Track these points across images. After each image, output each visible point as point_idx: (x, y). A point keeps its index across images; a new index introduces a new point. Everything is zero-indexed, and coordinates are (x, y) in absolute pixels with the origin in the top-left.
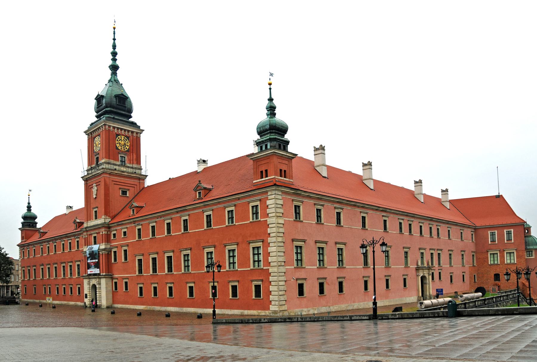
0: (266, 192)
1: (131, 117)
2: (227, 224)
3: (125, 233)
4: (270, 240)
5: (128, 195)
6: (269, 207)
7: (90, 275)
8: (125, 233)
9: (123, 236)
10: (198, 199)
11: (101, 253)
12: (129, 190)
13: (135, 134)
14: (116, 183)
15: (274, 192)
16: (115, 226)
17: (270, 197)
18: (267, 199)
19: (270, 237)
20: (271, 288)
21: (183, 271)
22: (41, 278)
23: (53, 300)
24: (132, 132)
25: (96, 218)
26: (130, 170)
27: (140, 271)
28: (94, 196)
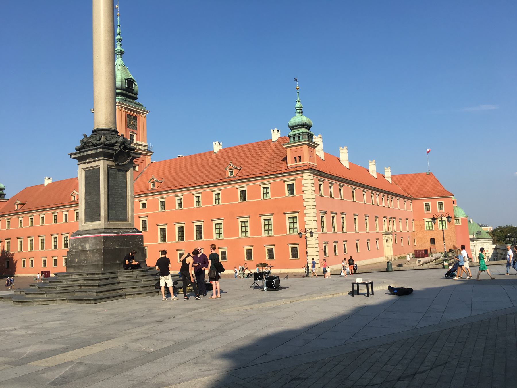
0: (302, 173)
1: (136, 99)
2: (262, 198)
3: (144, 205)
4: (305, 211)
5: (137, 169)
6: (305, 185)
9: (141, 207)
13: (142, 114)
15: (309, 174)
17: (304, 178)
18: (302, 179)
21: (215, 238)
22: (19, 250)
24: (140, 113)
27: (163, 239)
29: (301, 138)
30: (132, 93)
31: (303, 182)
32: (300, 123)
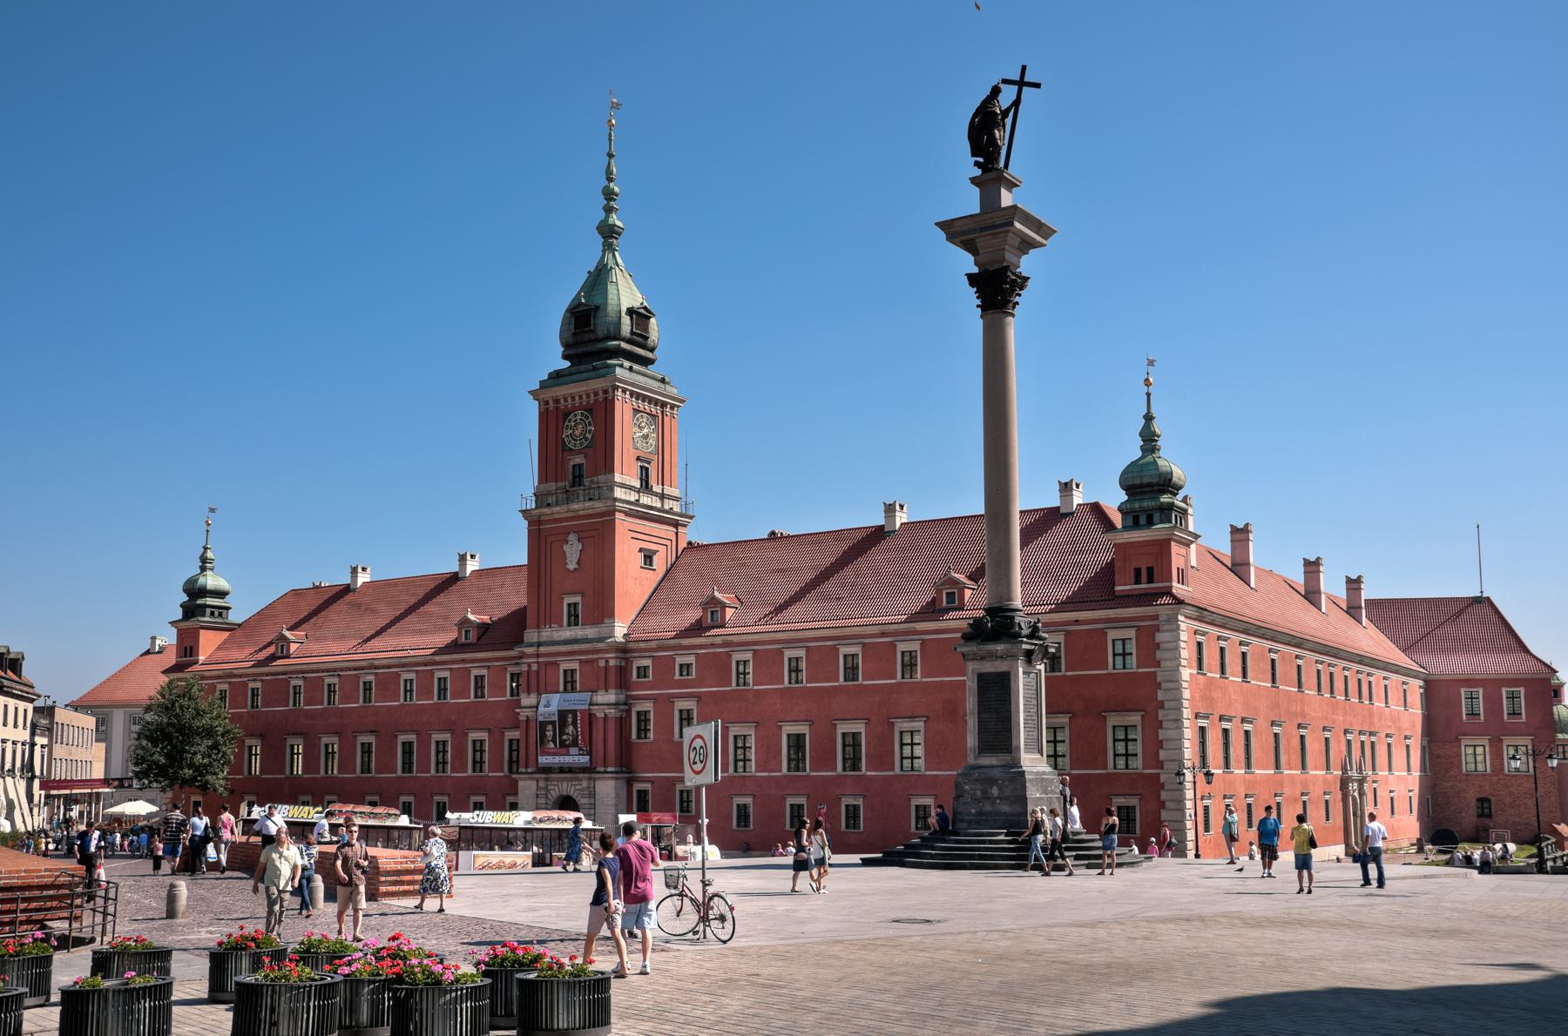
4: (1161, 713)
7: (547, 770)
8: (686, 668)
9: (677, 677)
10: (947, 610)
11: (600, 715)
12: (655, 552)
14: (636, 535)
18: (1157, 629)
19: (1162, 707)
20: (1164, 815)
21: (897, 770)
24: (664, 405)
25: (574, 620)
26: (657, 503)
28: (572, 566)
29: (1156, 517)
30: (644, 347)
31: (1160, 637)
32: (1155, 480)
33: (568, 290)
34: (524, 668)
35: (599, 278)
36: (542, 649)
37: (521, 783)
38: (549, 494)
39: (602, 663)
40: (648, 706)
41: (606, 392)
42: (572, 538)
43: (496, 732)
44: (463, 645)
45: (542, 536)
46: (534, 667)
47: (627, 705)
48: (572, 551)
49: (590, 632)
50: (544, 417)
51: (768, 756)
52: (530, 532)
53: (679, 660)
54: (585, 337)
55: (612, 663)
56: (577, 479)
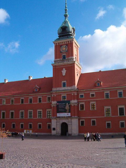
7: (59, 117)
8: (93, 95)
11: (73, 105)
16: (82, 92)
23: (33, 132)
28: (64, 75)
33: (60, 25)
34: (53, 96)
35: (65, 22)
36: (57, 92)
37: (52, 120)
38: (58, 61)
39: (73, 94)
40: (83, 103)
41: (71, 41)
42: (64, 69)
43: (44, 110)
44: (36, 92)
45: (56, 70)
46: (55, 96)
47: (78, 102)
48: (64, 72)
49: (69, 88)
50: (56, 47)
51: (114, 113)
52: (53, 68)
53: (91, 94)
54: (64, 32)
55: (75, 94)
56: (64, 57)
